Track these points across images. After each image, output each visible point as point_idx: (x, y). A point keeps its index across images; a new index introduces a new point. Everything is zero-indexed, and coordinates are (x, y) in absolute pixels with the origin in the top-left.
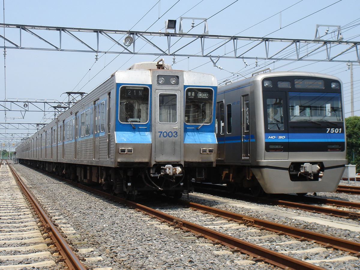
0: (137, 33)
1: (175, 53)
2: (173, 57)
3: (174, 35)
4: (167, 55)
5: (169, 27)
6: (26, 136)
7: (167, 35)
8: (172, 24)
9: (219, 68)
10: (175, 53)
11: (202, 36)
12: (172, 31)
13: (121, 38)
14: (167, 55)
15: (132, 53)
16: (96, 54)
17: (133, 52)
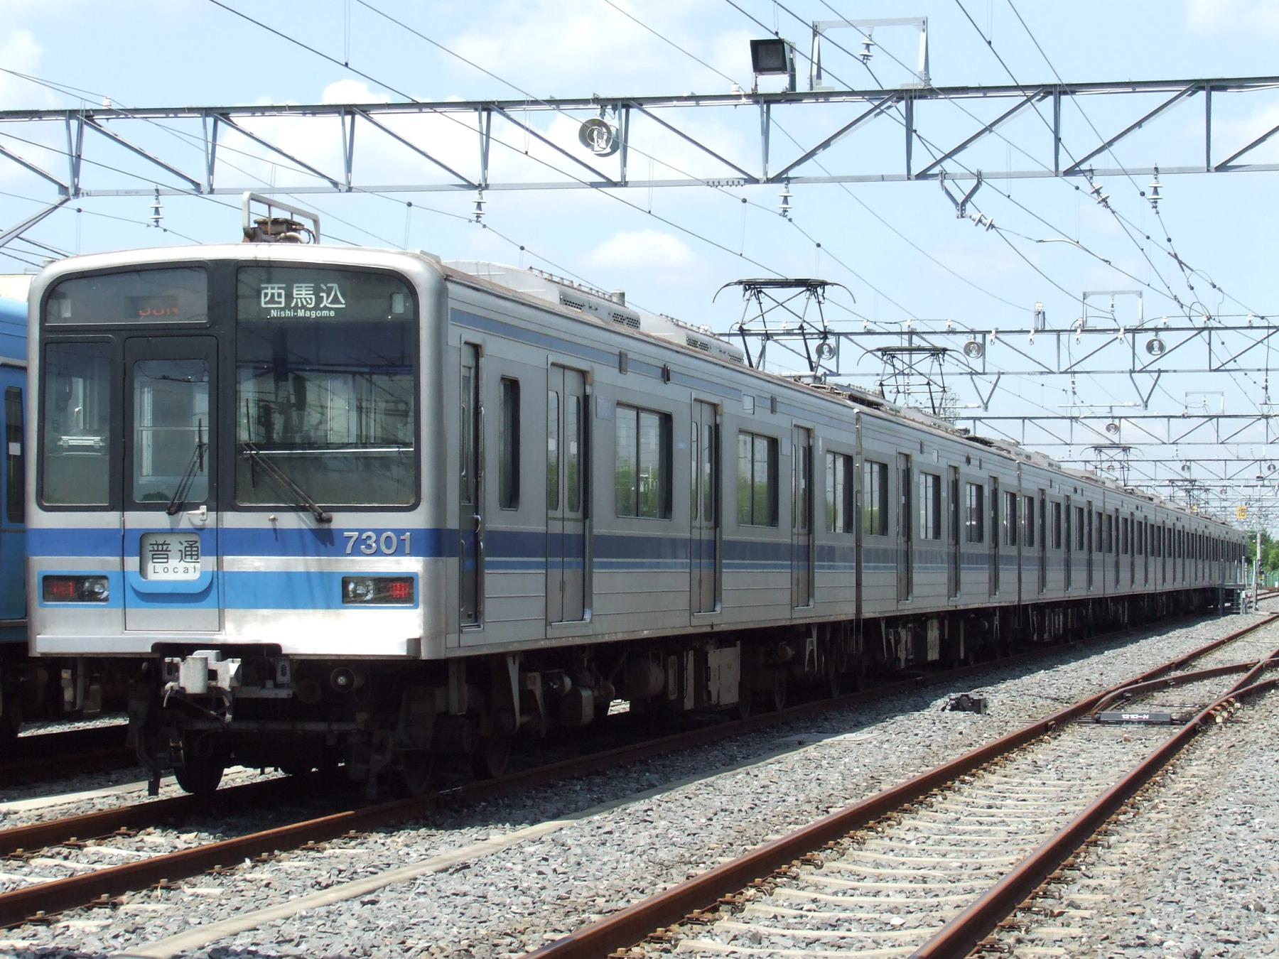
0: (627, 104)
1: (791, 174)
2: (780, 188)
3: (790, 96)
4: (756, 181)
5: (759, 67)
6: (1180, 470)
7: (755, 97)
8: (769, 54)
9: (980, 221)
10: (791, 174)
11: (907, 95)
12: (775, 83)
13: (565, 127)
14: (756, 181)
15: (615, 184)
16: (475, 194)
17: (616, 178)
